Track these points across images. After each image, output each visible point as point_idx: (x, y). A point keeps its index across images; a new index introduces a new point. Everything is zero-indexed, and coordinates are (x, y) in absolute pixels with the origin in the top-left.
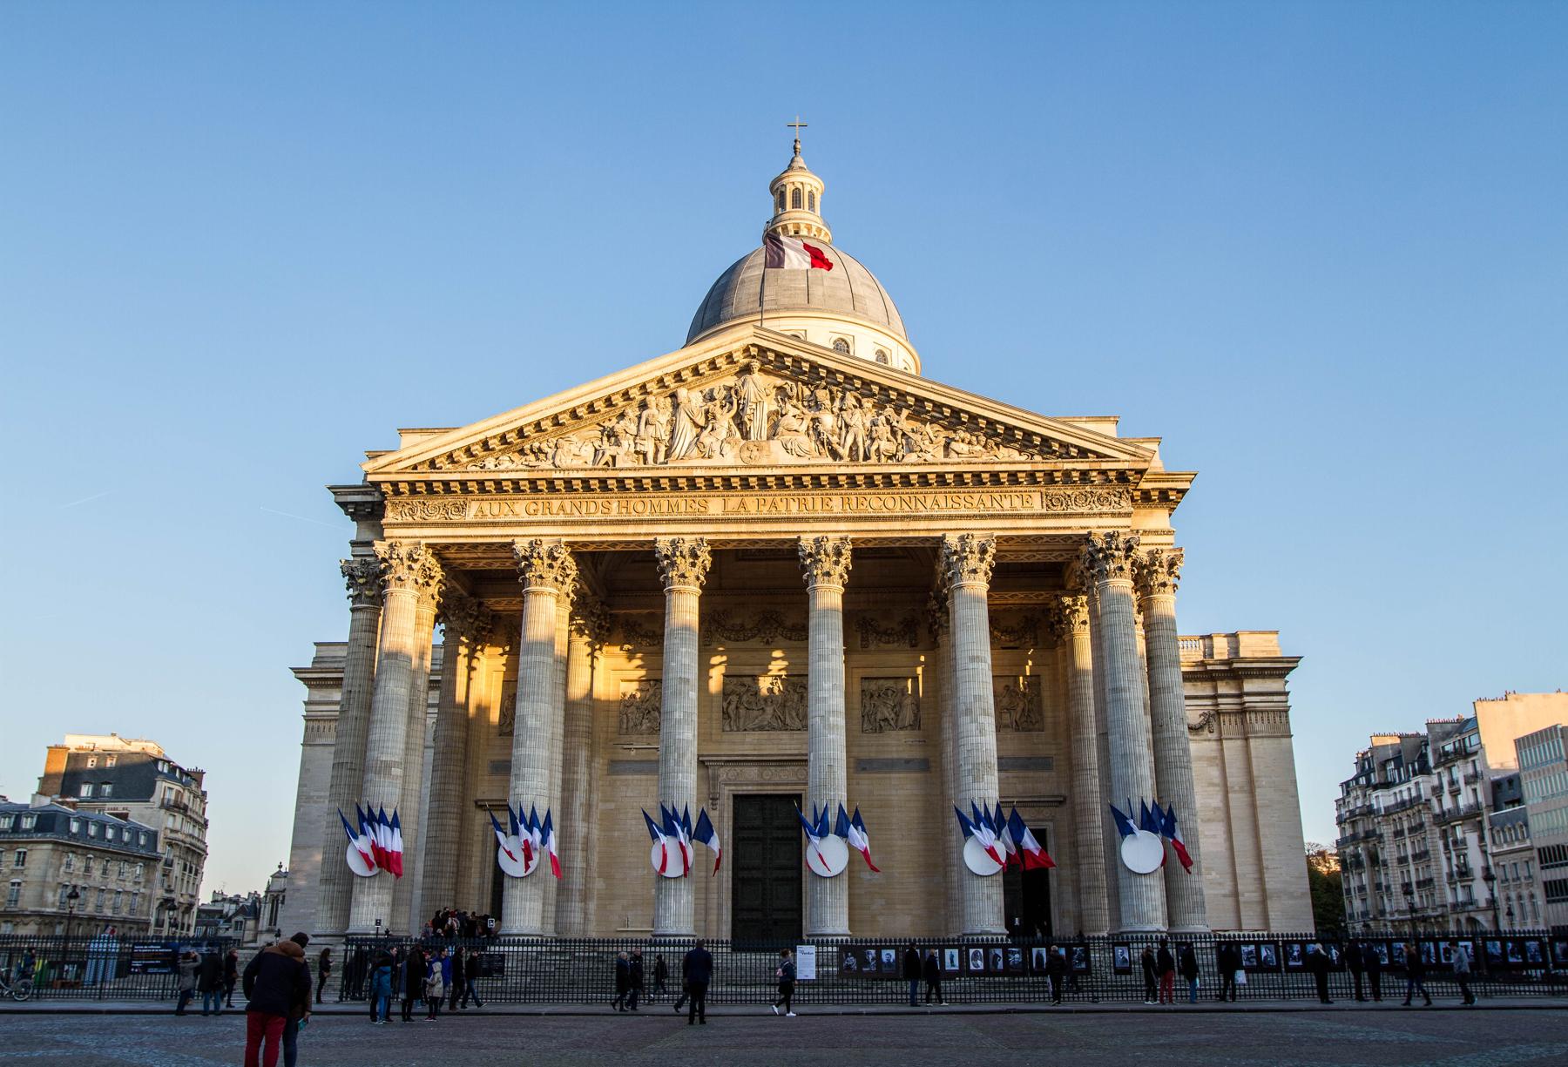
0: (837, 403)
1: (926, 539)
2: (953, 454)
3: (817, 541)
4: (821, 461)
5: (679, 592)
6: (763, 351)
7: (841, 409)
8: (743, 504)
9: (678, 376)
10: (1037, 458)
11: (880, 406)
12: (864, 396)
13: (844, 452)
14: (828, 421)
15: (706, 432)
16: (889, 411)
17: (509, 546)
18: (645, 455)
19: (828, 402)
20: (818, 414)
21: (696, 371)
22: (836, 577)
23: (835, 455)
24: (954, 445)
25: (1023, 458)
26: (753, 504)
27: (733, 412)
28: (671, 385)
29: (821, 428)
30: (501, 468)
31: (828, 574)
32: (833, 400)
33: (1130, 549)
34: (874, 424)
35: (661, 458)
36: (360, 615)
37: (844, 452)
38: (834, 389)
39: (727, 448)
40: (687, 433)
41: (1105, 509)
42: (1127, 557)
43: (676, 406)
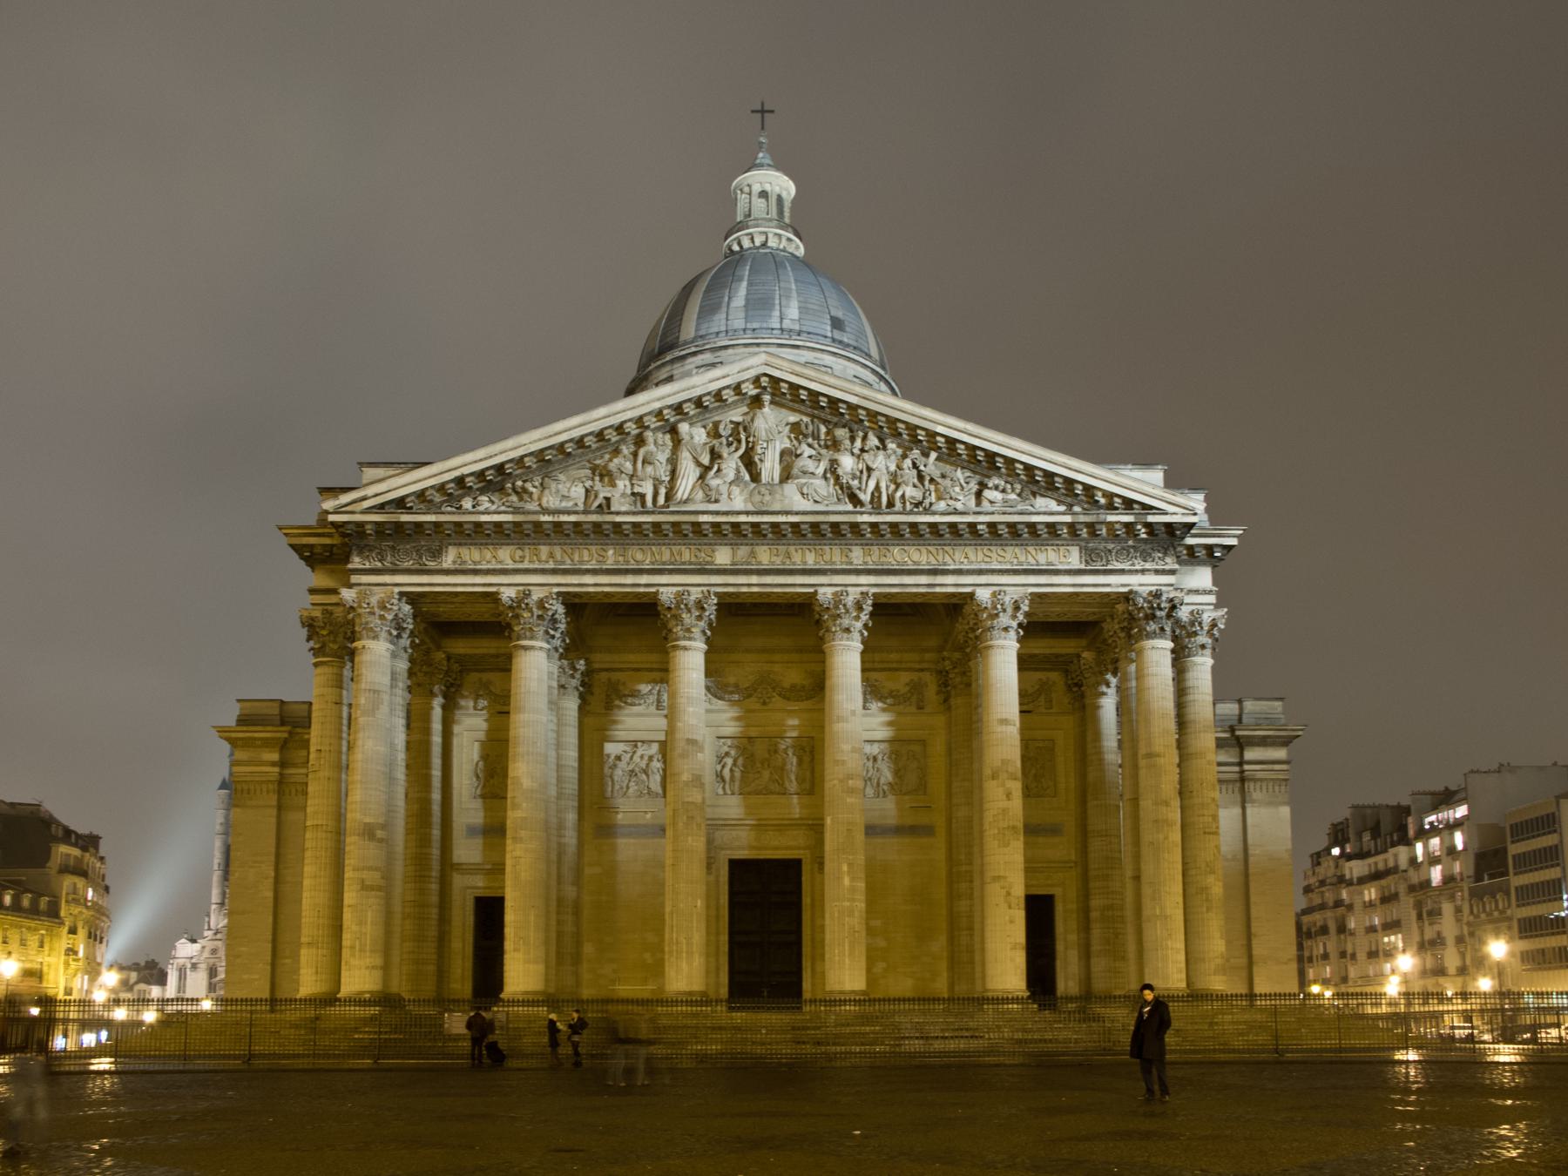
0: (858, 444)
1: (953, 595)
2: (985, 504)
3: (835, 594)
4: (841, 508)
5: (685, 648)
6: (776, 381)
7: (862, 450)
8: (753, 554)
9: (678, 408)
10: (1077, 509)
14: (847, 463)
16: (916, 453)
17: (493, 598)
18: (643, 496)
19: (847, 442)
20: (836, 456)
21: (698, 402)
22: (857, 636)
24: (987, 493)
25: (1062, 508)
26: (765, 555)
29: (840, 472)
30: (481, 508)
31: (848, 630)
33: (1174, 607)
34: (899, 467)
35: (661, 500)
36: (320, 670)
37: (865, 497)
38: (856, 427)
41: (1148, 566)
42: (1169, 616)
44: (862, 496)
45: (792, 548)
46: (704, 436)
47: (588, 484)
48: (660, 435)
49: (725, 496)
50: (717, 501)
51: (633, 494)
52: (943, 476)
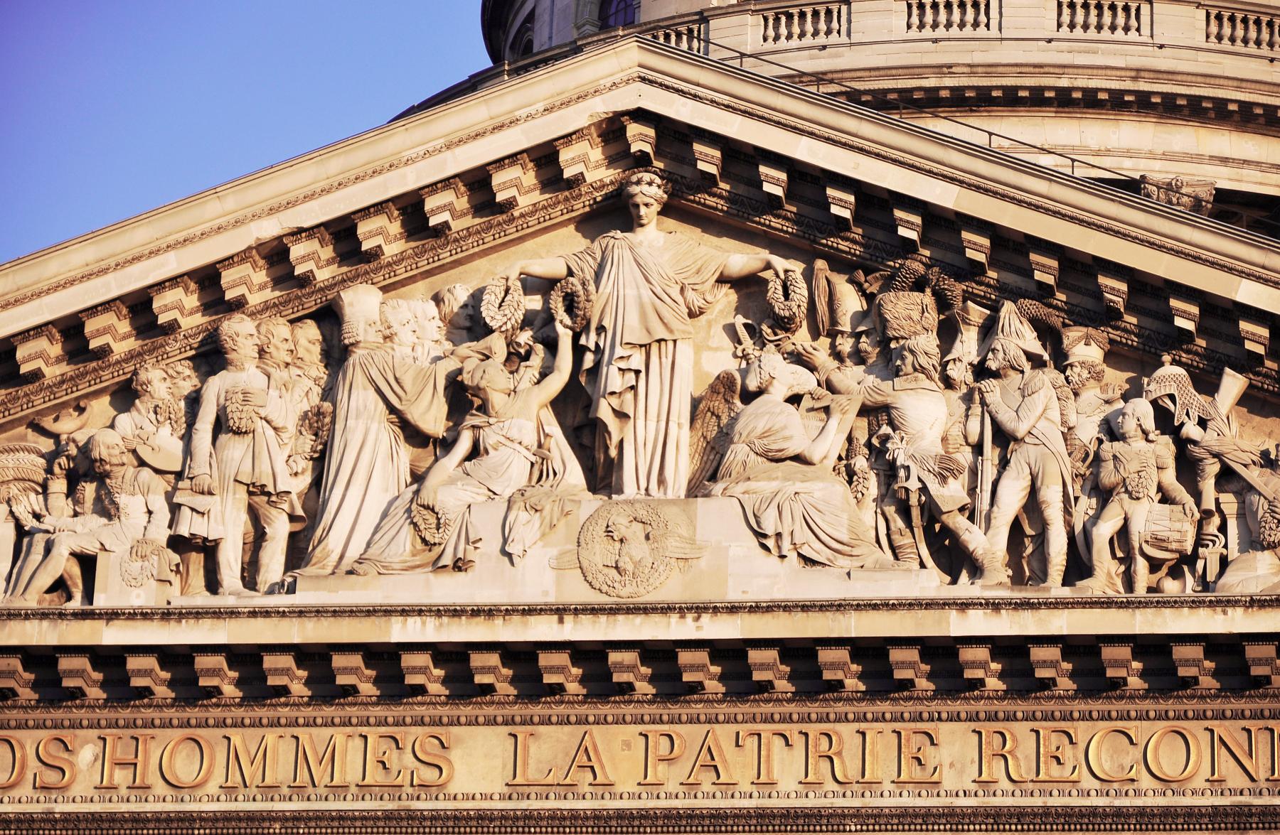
0: (967, 346)
6: (675, 137)
7: (981, 371)
11: (1136, 359)
12: (1080, 317)
13: (988, 543)
18: (209, 550)
19: (928, 342)
20: (886, 391)
23: (954, 557)
28: (312, 280)
29: (899, 451)
32: (948, 333)
34: (1111, 430)
39: (526, 527)
40: (372, 465)
43: (336, 354)
44: (974, 538)
45: (723, 734)
46: (434, 329)
47: (27, 504)
48: (281, 329)
49: (492, 544)
50: (459, 565)
51: (178, 544)
52: (1267, 461)
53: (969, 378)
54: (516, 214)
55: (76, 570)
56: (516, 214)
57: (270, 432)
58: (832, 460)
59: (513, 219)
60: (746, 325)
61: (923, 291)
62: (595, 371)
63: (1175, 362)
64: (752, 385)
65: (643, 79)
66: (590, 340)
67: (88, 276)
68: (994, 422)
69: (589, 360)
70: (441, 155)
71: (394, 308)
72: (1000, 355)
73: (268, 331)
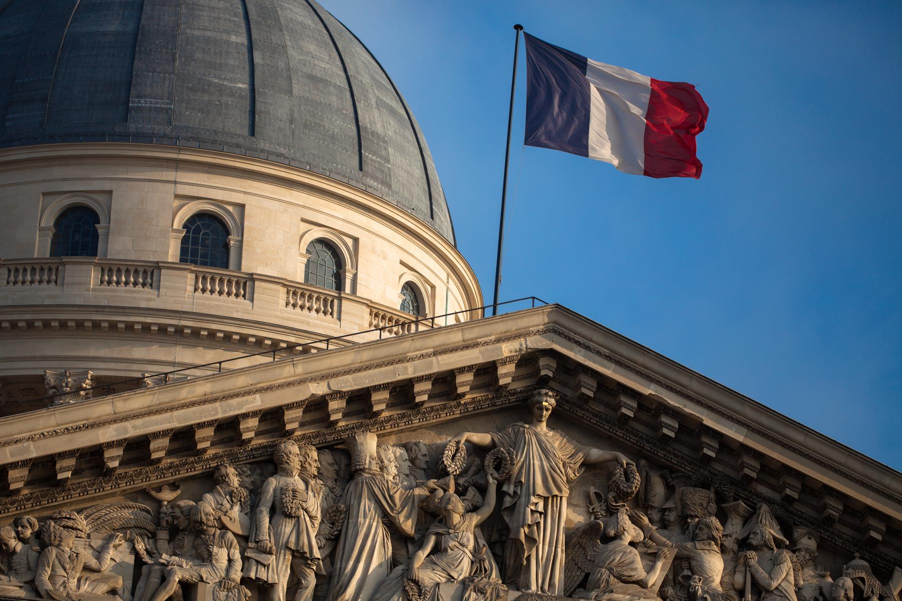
7: (744, 544)
9: (359, 402)
15: (422, 555)
16: (860, 568)
27: (487, 511)
48: (314, 454)
53: (735, 547)
54: (462, 402)
55: (181, 591)
56: (462, 402)
57: (307, 519)
58: (657, 588)
59: (459, 404)
60: (596, 493)
61: (709, 490)
62: (512, 508)
63: (862, 558)
64: (612, 533)
65: (555, 331)
66: (510, 488)
67: (205, 402)
68: (753, 577)
69: (508, 501)
70: (430, 359)
71: (385, 450)
72: (759, 537)
73: (306, 453)
